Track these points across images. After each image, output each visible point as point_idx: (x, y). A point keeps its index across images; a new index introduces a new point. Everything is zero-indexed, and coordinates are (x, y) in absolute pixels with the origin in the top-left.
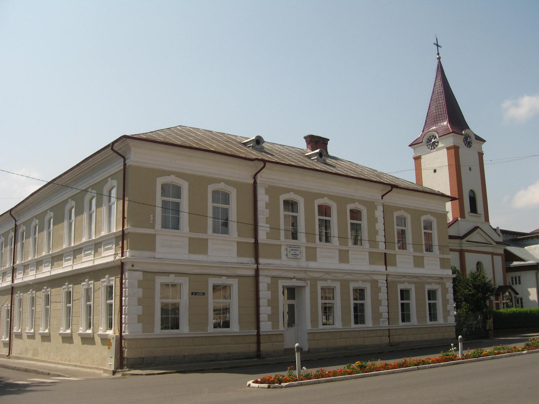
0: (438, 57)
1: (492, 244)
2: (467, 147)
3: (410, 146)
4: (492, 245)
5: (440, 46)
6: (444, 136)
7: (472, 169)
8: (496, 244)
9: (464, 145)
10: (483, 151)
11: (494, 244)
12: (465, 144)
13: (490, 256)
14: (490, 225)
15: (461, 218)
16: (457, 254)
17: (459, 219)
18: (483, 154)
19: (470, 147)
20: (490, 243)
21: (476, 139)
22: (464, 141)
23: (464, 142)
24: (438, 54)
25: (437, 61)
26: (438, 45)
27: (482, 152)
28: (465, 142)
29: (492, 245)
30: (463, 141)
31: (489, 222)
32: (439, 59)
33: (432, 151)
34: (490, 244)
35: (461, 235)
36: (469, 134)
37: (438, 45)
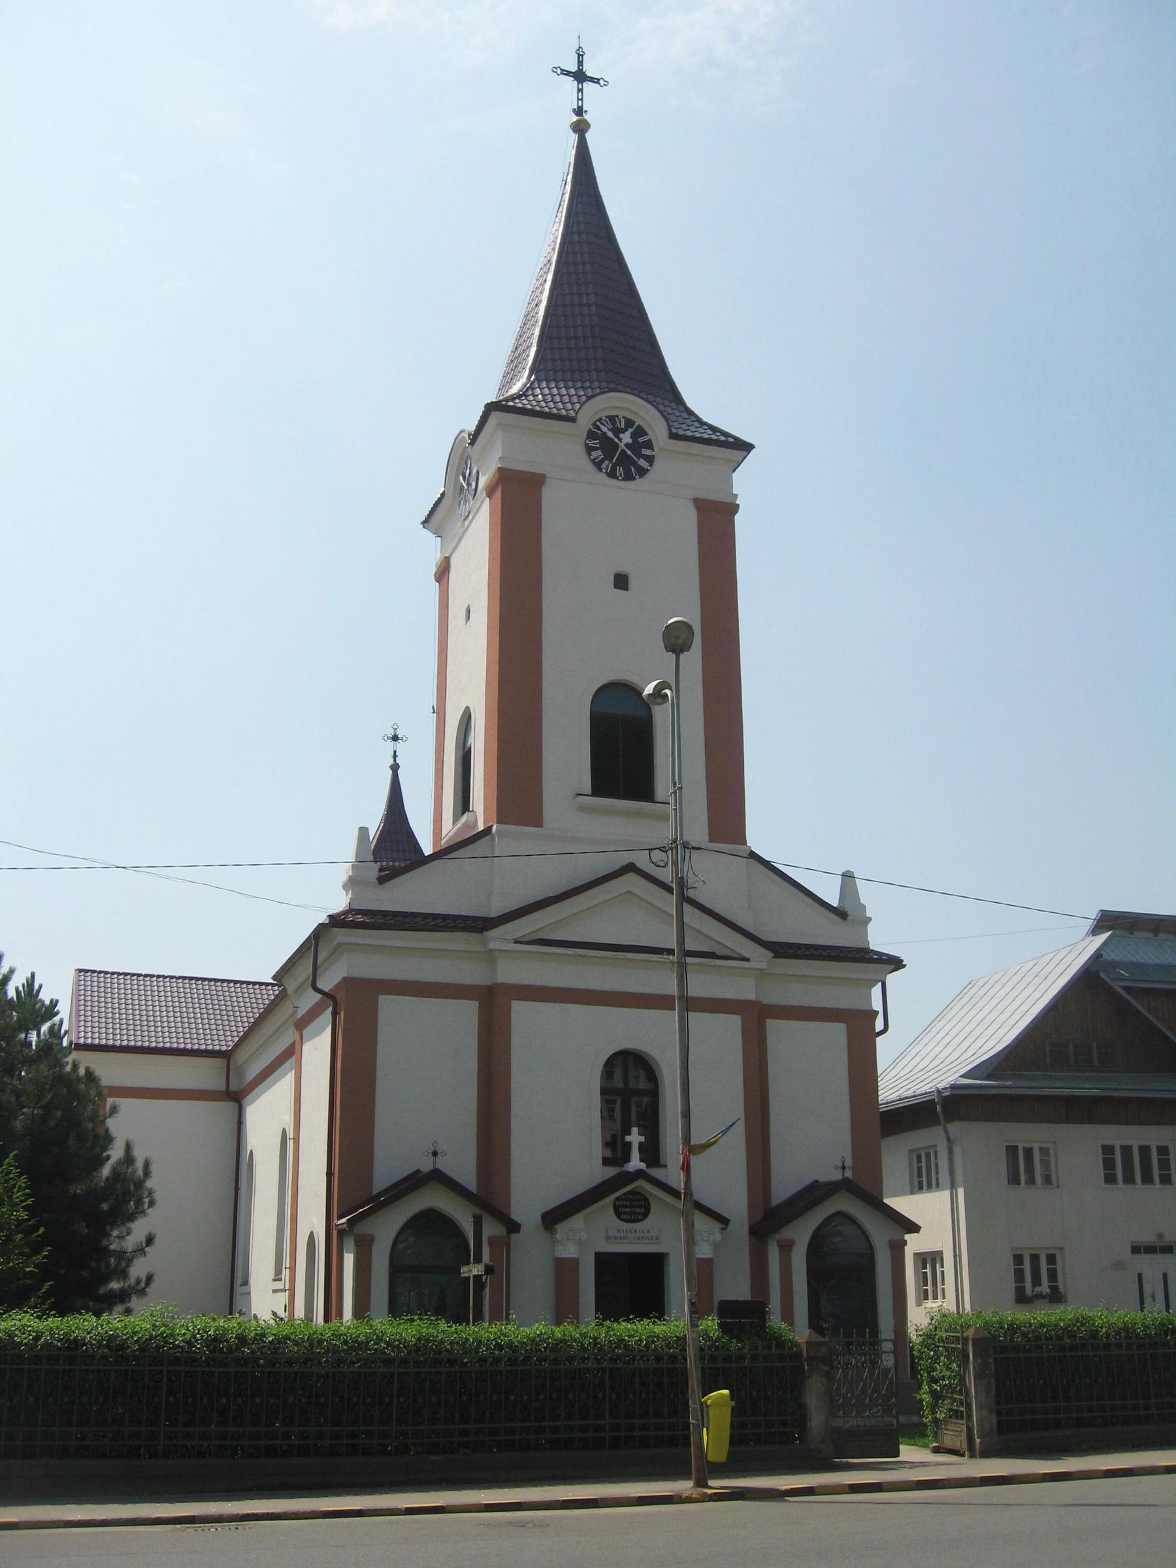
0: (575, 118)
1: (747, 955)
2: (612, 474)
3: (426, 522)
4: (748, 960)
5: (596, 81)
6: (481, 436)
7: (632, 583)
8: (773, 955)
9: (590, 467)
10: (736, 495)
11: (760, 958)
12: (598, 465)
13: (733, 1023)
14: (753, 855)
15: (497, 823)
16: (470, 1009)
17: (494, 828)
18: (735, 508)
19: (629, 477)
20: (735, 951)
21: (673, 436)
22: (589, 450)
23: (590, 455)
24: (579, 111)
25: (574, 138)
26: (580, 76)
27: (729, 500)
28: (597, 454)
29: (748, 960)
30: (582, 451)
31: (744, 842)
32: (581, 128)
33: (467, 523)
34: (740, 956)
35: (495, 909)
36: (629, 416)
37: (580, 76)
